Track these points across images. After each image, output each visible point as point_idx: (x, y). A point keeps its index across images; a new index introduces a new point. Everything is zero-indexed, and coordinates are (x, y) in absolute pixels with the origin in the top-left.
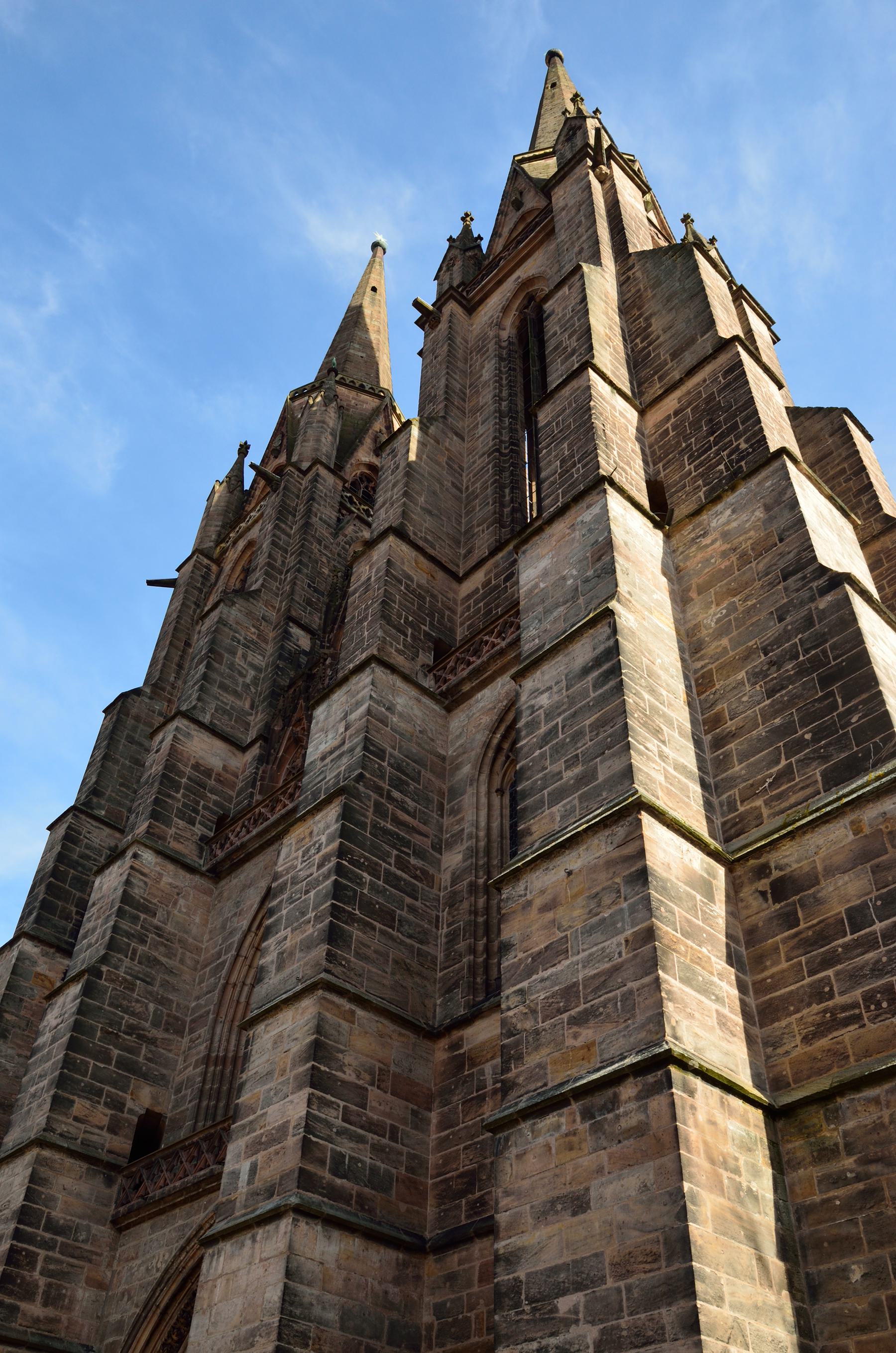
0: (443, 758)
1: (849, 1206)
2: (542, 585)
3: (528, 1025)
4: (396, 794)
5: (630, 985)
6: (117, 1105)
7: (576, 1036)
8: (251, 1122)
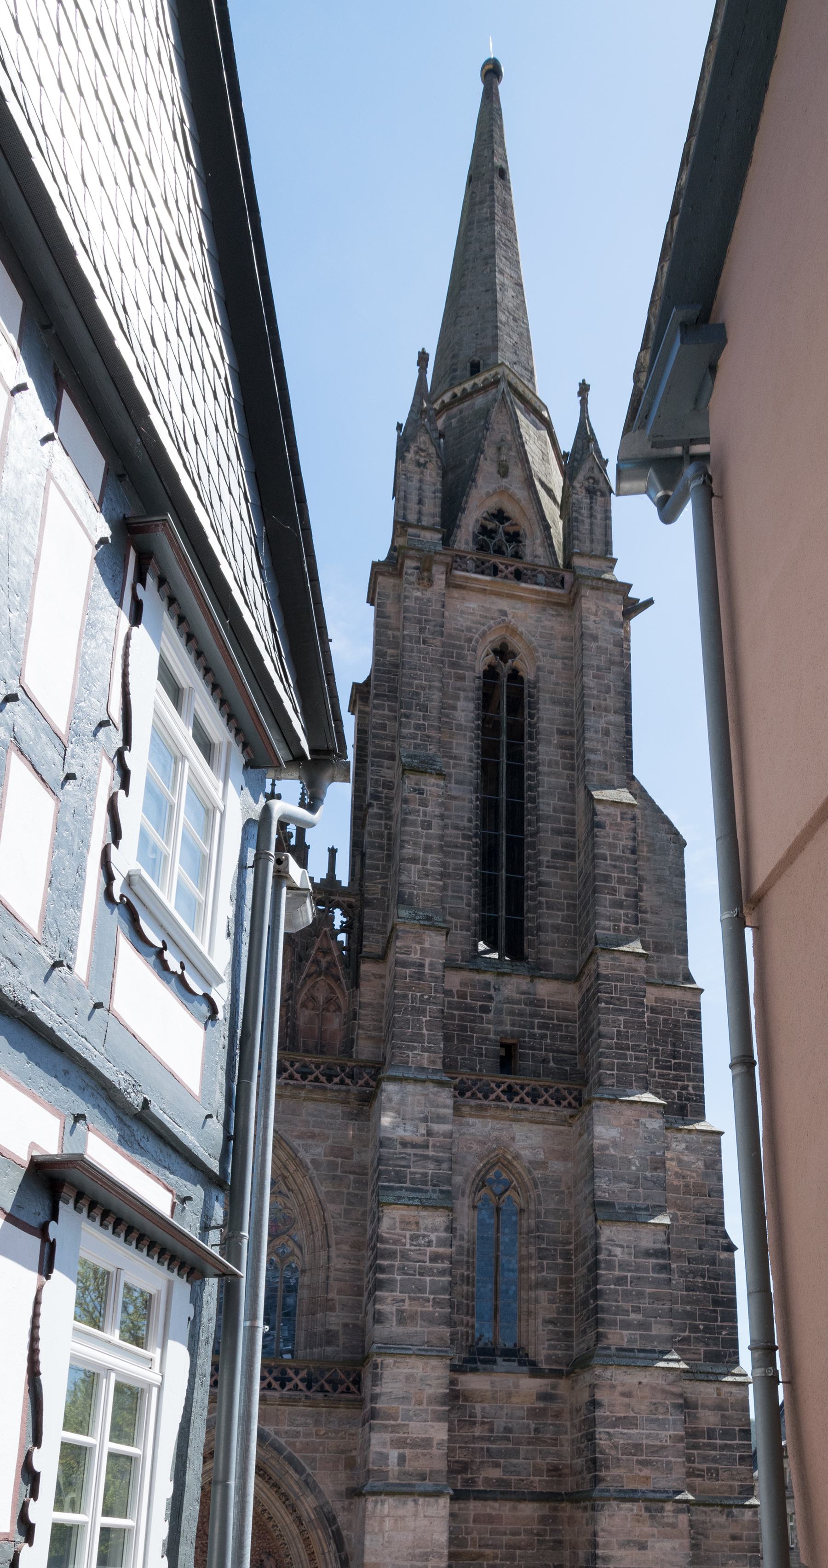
2: (612, 1151)
3: (613, 1452)
5: (673, 1460)
7: (640, 1470)
8: (392, 1426)
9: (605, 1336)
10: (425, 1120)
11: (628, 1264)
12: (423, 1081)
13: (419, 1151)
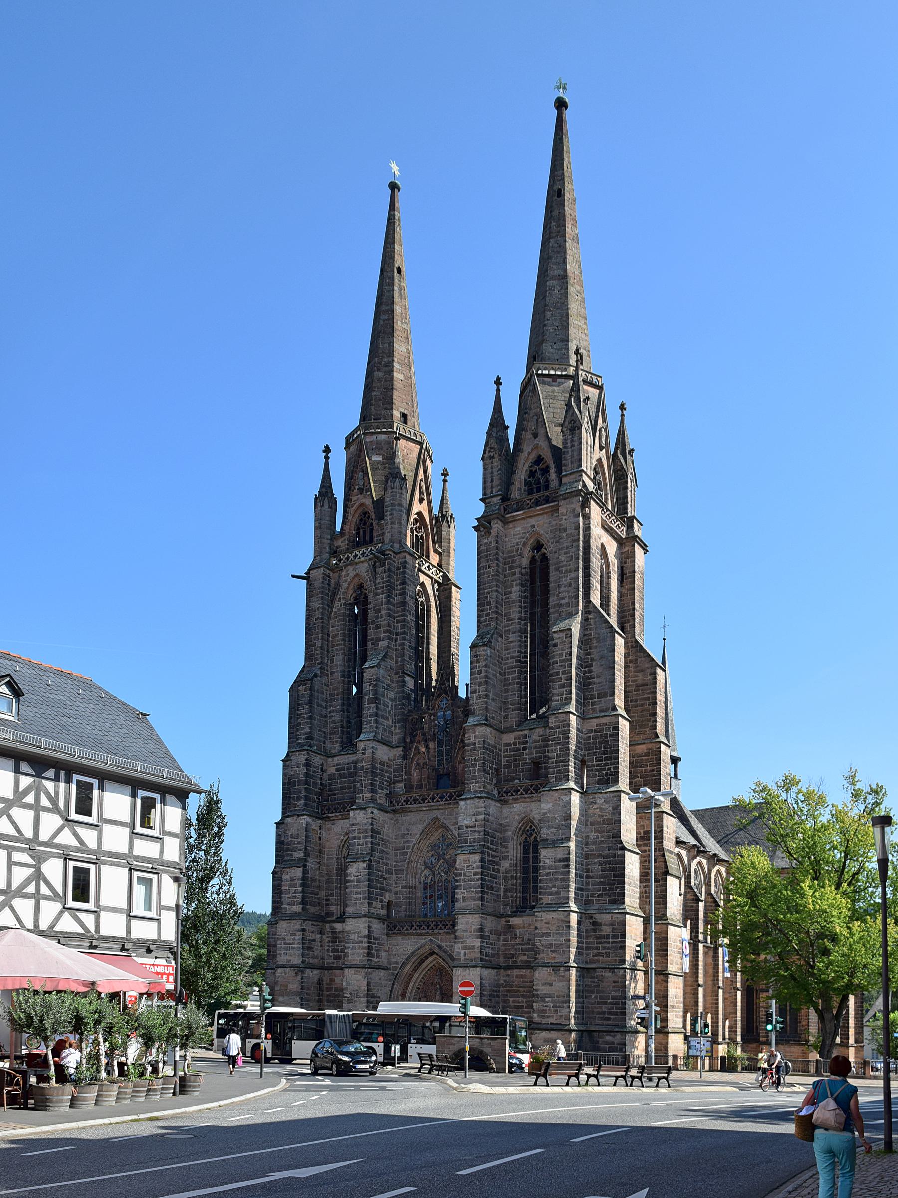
0: (501, 825)
1: (594, 986)
4: (492, 846)
6: (382, 901)
9: (541, 899)
10: (474, 815)
11: (552, 866)
12: (473, 798)
13: (472, 829)
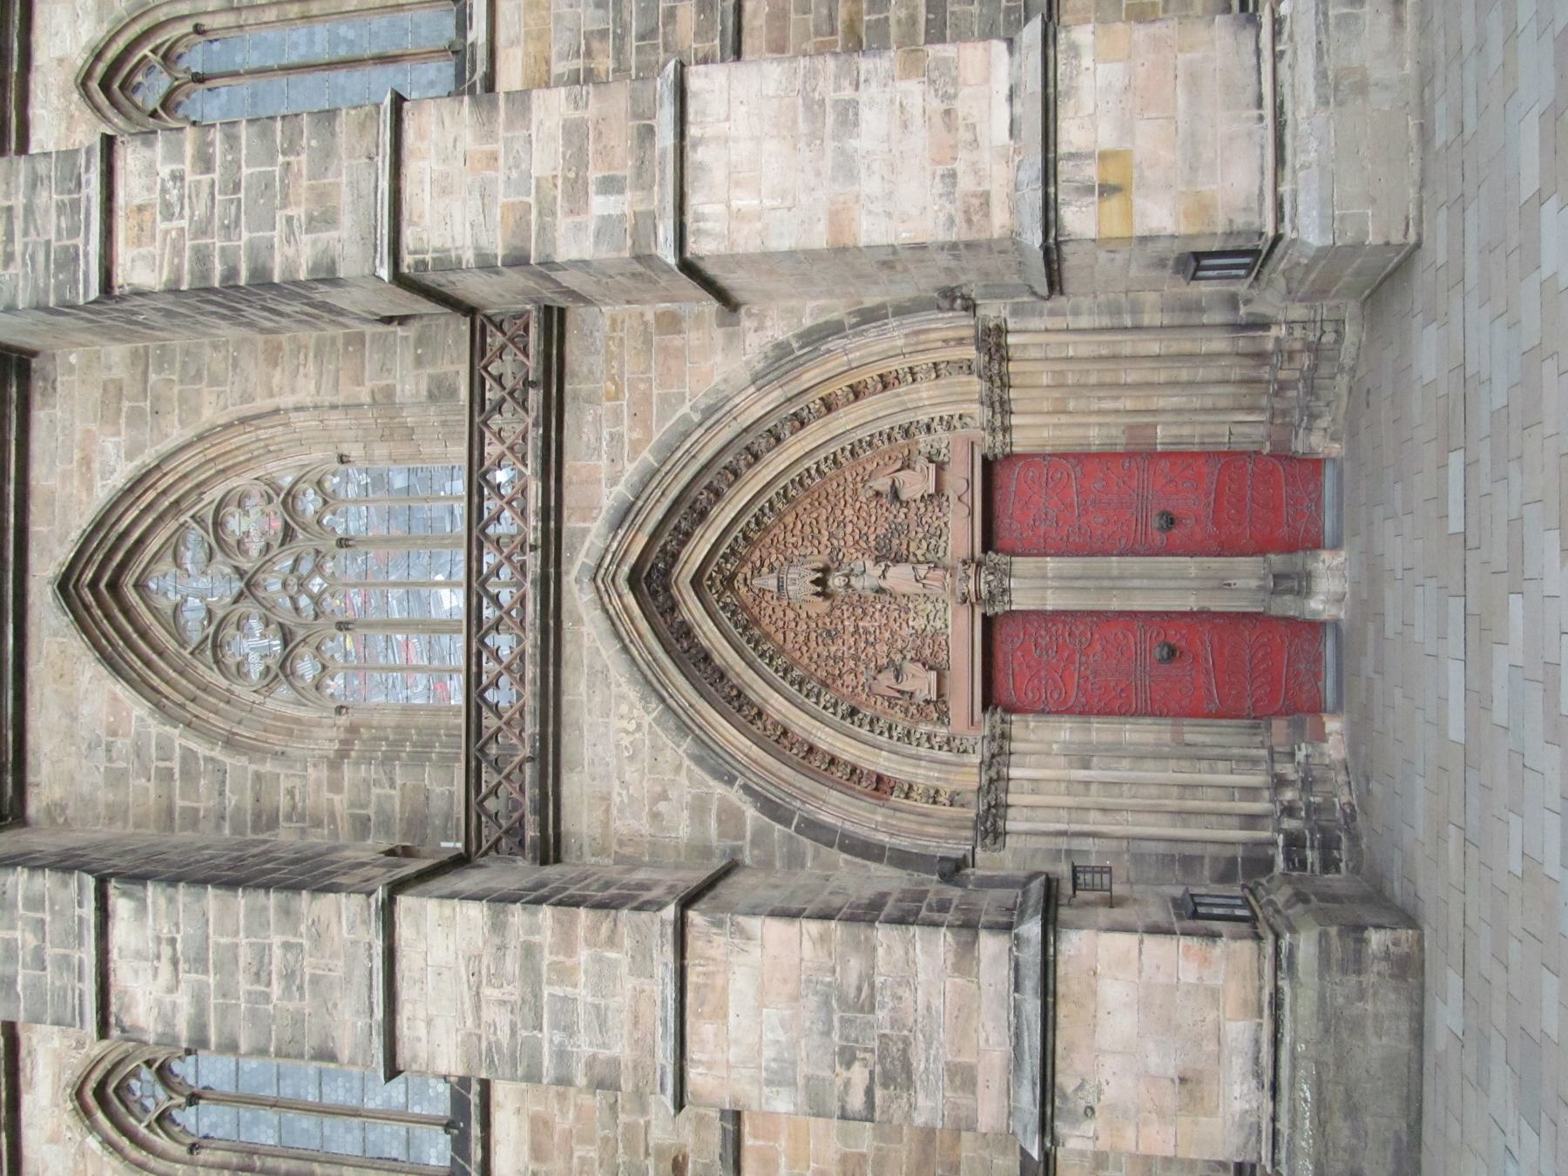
13: (18, 226)
